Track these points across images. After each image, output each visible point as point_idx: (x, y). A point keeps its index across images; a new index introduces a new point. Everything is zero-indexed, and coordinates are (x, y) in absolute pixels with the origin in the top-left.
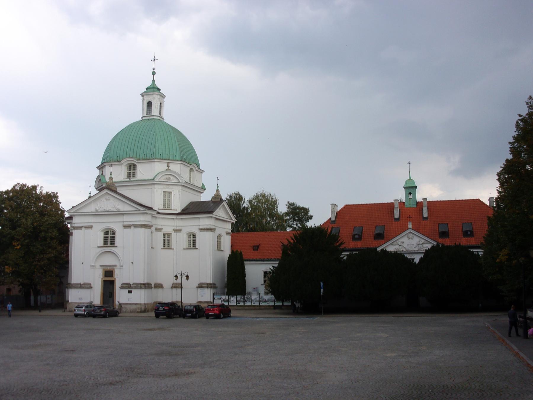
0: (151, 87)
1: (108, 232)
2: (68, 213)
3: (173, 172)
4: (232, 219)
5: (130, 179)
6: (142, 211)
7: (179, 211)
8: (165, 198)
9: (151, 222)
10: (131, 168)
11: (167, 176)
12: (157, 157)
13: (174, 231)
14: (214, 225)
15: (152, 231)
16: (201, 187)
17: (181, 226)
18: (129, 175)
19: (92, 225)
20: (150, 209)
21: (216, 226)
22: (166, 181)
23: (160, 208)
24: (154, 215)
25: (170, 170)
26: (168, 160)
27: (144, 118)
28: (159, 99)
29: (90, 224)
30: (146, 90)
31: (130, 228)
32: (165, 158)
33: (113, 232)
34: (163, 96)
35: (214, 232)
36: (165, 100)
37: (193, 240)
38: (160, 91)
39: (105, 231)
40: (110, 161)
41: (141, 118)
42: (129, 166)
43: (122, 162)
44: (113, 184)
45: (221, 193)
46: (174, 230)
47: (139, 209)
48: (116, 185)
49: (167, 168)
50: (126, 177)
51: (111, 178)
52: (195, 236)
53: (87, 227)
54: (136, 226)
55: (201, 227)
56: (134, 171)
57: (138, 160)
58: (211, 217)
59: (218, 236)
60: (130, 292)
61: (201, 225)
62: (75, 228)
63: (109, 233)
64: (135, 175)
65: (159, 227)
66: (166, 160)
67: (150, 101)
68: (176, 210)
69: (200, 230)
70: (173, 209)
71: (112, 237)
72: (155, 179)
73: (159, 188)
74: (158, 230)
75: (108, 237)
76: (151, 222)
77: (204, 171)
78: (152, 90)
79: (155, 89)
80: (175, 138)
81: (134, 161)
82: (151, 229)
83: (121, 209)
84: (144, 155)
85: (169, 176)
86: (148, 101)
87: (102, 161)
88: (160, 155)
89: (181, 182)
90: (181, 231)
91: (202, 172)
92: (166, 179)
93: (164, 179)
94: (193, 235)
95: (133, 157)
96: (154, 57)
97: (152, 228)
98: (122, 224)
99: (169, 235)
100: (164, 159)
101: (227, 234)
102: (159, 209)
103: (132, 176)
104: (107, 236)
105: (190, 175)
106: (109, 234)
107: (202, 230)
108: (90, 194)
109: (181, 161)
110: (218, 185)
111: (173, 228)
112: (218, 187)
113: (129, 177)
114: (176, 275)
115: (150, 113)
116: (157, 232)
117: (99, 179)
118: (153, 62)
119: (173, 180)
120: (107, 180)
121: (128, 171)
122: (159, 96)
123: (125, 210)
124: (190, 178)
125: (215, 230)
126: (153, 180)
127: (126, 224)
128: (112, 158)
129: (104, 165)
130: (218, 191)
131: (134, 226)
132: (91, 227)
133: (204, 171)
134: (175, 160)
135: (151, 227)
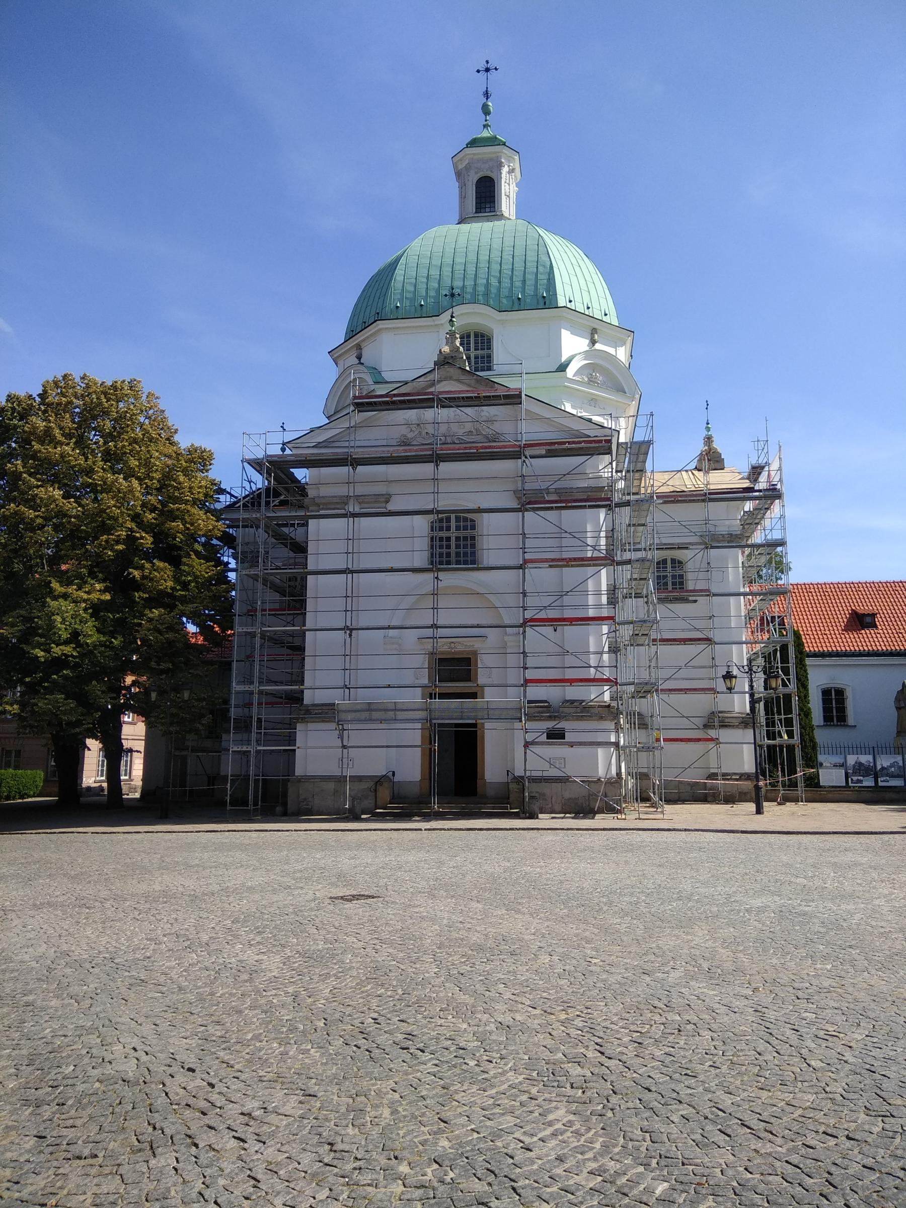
1: (448, 520)
37: (674, 577)
60: (556, 735)
63: (453, 524)
75: (448, 539)
86: (481, 175)
96: (487, 62)
104: (444, 534)
110: (708, 424)
112: (708, 429)
114: (728, 672)
118: (483, 75)
130: (709, 440)
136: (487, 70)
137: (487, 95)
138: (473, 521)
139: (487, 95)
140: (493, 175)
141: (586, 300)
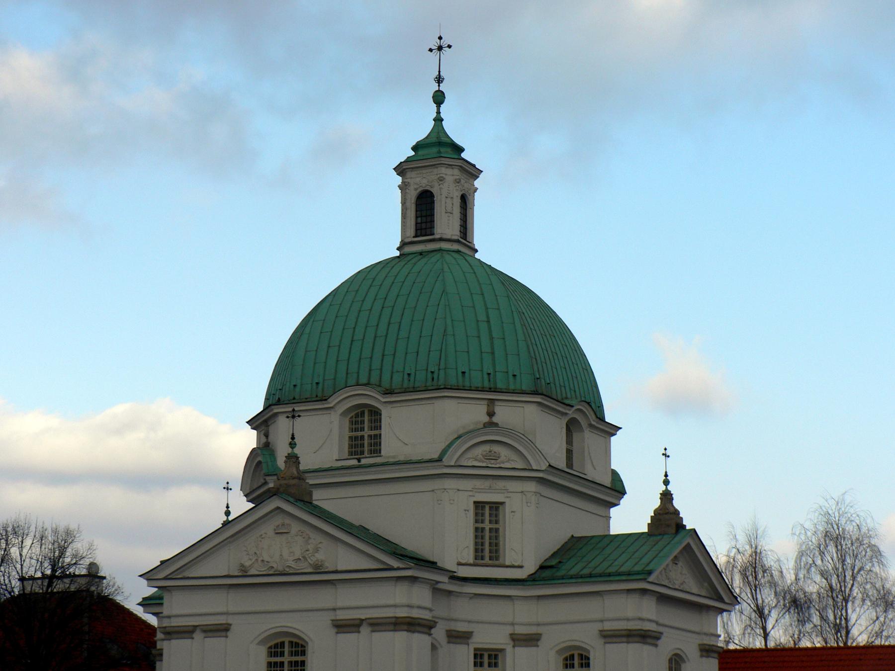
0: (434, 140)
1: (282, 644)
2: (148, 580)
3: (509, 432)
4: (720, 599)
5: (359, 460)
6: (398, 569)
7: (530, 568)
8: (480, 525)
9: (431, 610)
10: (363, 422)
11: (486, 448)
12: (453, 381)
13: (512, 643)
14: (654, 618)
15: (437, 645)
16: (609, 486)
17: (538, 625)
18: (356, 447)
19: (230, 622)
20: (431, 565)
21: (661, 621)
22: (484, 465)
23: (463, 562)
24: (440, 586)
25: (496, 425)
26: (490, 390)
27: (408, 249)
28: (458, 181)
29: (221, 620)
30: (413, 153)
31: (359, 632)
32: (480, 385)
33: (299, 647)
34: (472, 172)
35: (656, 646)
36: (477, 183)
38: (463, 155)
39: (272, 643)
40: (294, 401)
41: (398, 249)
42: (357, 416)
43: (332, 402)
44: (301, 476)
45: (677, 504)
46: (515, 637)
47: (388, 565)
48: (311, 482)
49: (486, 419)
50: (346, 456)
51: (293, 459)
52: (589, 659)
53: (211, 631)
54: (377, 625)
55: (608, 626)
56: (373, 433)
57: (389, 392)
58: (644, 591)
59: (670, 660)
61: (340, 609)
62: (171, 633)
64: (376, 449)
65: (462, 627)
66: (482, 390)
67: (428, 188)
68: (521, 567)
69: (605, 637)
70: (507, 563)
71: (296, 662)
72: (444, 460)
73: (458, 490)
74: (458, 637)
76: (431, 610)
77: (620, 428)
78: (435, 150)
79: (442, 150)
80: (515, 314)
81: (374, 398)
82: (430, 635)
83: (327, 564)
84: (406, 376)
85: (496, 448)
86: (421, 189)
87: (267, 399)
88: (460, 374)
89: (535, 468)
90: (539, 643)
91: (613, 432)
92: (483, 456)
93: (476, 460)
94: (581, 656)
95: (368, 384)
97: (433, 631)
98: (331, 616)
99: (496, 656)
100: (477, 390)
101: (704, 654)
102: (459, 564)
103: (366, 448)
104: (278, 659)
105: (569, 441)
106: (286, 653)
107: (609, 636)
108: (228, 513)
109: (535, 393)
110: (666, 475)
111: (509, 630)
112: (666, 482)
113: (356, 453)
115: (428, 231)
116: (451, 645)
117: (256, 462)
118: (435, 55)
119: (508, 461)
120: (281, 462)
121: (355, 434)
122: (456, 172)
123: (340, 568)
124: (569, 453)
125: (658, 638)
126: (439, 463)
127: (342, 615)
128: (298, 389)
129: (271, 414)
130: (667, 496)
131: (372, 625)
132: (223, 630)
133: (620, 428)
134: (514, 392)
135: (431, 628)
136: (440, 48)
137: (439, 80)
138: (302, 646)
139: (439, 80)
140: (435, 191)
141: (488, 368)
